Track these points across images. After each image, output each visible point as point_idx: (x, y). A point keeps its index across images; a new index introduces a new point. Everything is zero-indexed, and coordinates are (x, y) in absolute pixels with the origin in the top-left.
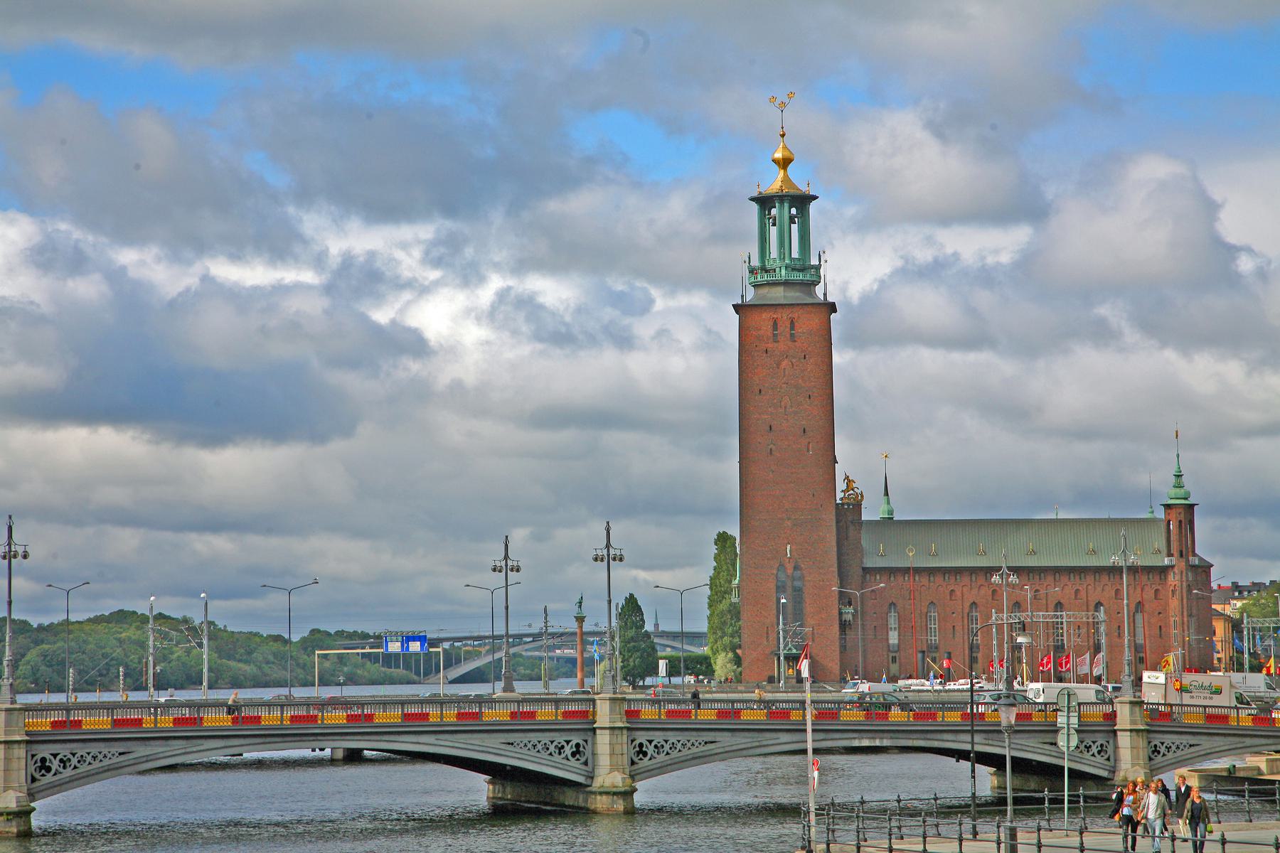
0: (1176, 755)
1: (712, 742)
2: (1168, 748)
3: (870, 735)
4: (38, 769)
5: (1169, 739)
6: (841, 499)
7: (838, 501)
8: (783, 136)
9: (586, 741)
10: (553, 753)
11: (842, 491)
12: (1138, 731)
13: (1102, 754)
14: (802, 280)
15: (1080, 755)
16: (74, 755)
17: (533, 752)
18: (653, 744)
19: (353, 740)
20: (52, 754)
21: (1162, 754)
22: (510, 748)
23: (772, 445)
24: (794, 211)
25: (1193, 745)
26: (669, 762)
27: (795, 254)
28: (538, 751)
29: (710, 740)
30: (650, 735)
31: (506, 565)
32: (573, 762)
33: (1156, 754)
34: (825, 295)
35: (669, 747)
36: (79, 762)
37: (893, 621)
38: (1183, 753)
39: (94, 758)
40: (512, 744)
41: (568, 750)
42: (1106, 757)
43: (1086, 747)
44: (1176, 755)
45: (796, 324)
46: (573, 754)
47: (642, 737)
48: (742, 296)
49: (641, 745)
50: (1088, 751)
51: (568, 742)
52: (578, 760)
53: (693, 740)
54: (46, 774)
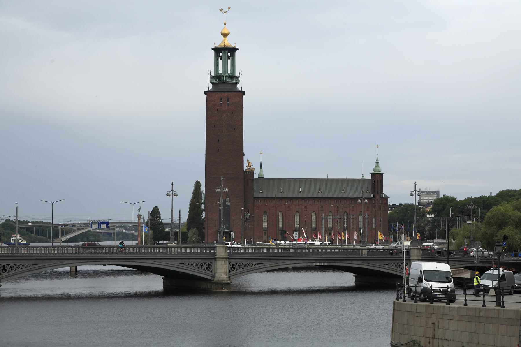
1: (260, 264)
3: (320, 261)
4: (2, 270)
6: (246, 170)
8: (225, 24)
9: (212, 263)
10: (199, 268)
11: (246, 167)
14: (232, 82)
15: (397, 269)
16: (15, 265)
17: (192, 267)
18: (238, 264)
19: (126, 261)
20: (7, 264)
22: (183, 265)
24: (229, 54)
26: (244, 271)
27: (229, 71)
28: (193, 267)
29: (259, 263)
30: (237, 261)
31: (172, 194)
32: (207, 271)
35: (243, 266)
36: (17, 268)
37: (265, 218)
39: (23, 266)
40: (183, 264)
41: (205, 267)
43: (399, 265)
45: (229, 99)
46: (207, 268)
47: (233, 262)
49: (233, 265)
50: (400, 267)
51: (205, 263)
52: (209, 270)
53: (253, 263)
54: (5, 272)
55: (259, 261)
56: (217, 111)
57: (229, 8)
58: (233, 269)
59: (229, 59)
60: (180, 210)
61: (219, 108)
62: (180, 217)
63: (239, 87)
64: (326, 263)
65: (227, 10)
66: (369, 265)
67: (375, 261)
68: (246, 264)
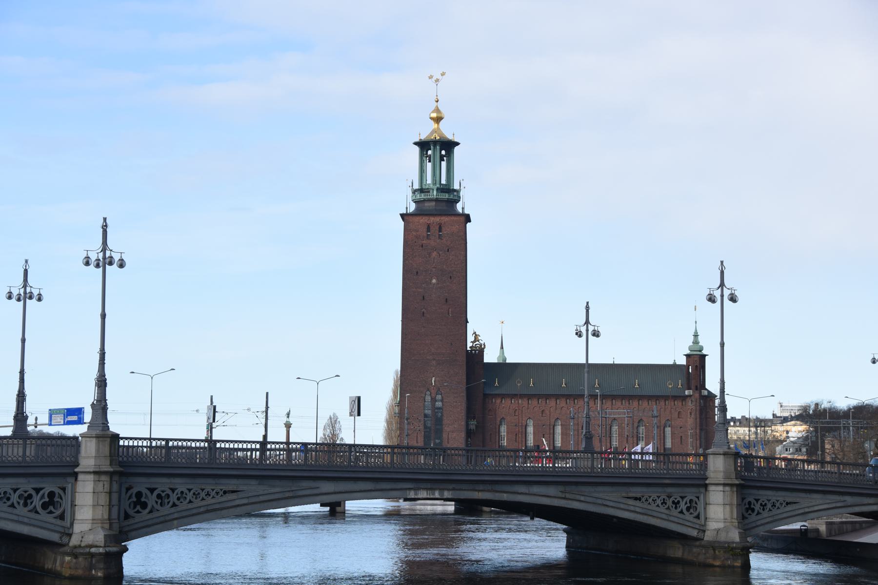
0: (771, 514)
1: (233, 492)
2: (764, 506)
3: (429, 485)
5: (764, 495)
6: (471, 347)
7: (469, 349)
8: (437, 101)
12: (731, 485)
13: (692, 511)
15: (667, 512)
18: (156, 493)
21: (756, 512)
23: (424, 310)
24: (443, 152)
26: (176, 515)
27: (444, 182)
29: (231, 488)
32: (44, 516)
33: (750, 512)
34: (463, 208)
38: (779, 511)
41: (37, 501)
42: (696, 514)
43: (673, 502)
44: (771, 514)
45: (443, 228)
46: (45, 506)
47: (141, 485)
48: (407, 208)
50: (676, 508)
52: (51, 512)
53: (208, 488)
55: (231, 485)
56: (421, 248)
57: (443, 74)
58: (138, 508)
59: (444, 160)
60: (267, 394)
61: (424, 242)
62: (267, 407)
63: (459, 207)
64: (448, 490)
65: (439, 77)
66: (582, 498)
67: (601, 489)
68: (186, 491)
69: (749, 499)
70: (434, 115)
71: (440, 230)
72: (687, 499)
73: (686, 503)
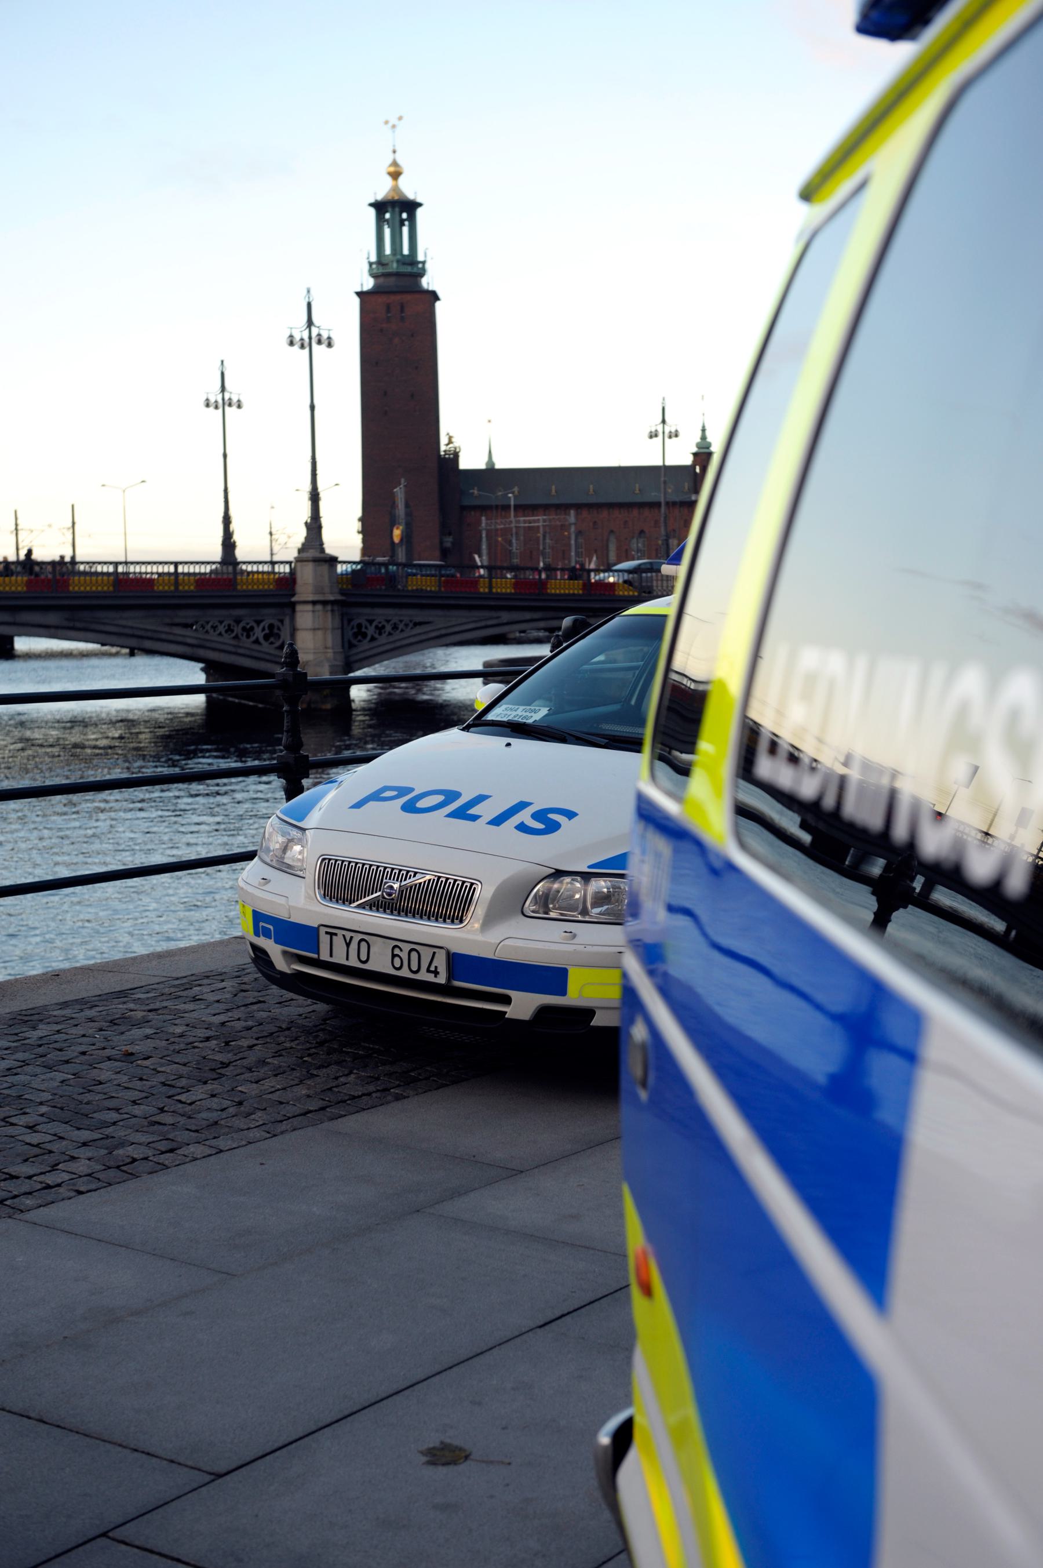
0: (391, 639)
2: (380, 629)
5: (380, 614)
6: (445, 451)
7: (442, 453)
8: (394, 152)
12: (324, 603)
21: (369, 638)
24: (404, 216)
25: (420, 624)
27: (406, 251)
34: (428, 284)
38: (402, 635)
43: (244, 629)
48: (362, 285)
50: (248, 637)
57: (400, 118)
62: (74, 523)
65: (396, 122)
69: (362, 620)
70: (392, 169)
71: (402, 310)
72: (265, 623)
73: (263, 629)
